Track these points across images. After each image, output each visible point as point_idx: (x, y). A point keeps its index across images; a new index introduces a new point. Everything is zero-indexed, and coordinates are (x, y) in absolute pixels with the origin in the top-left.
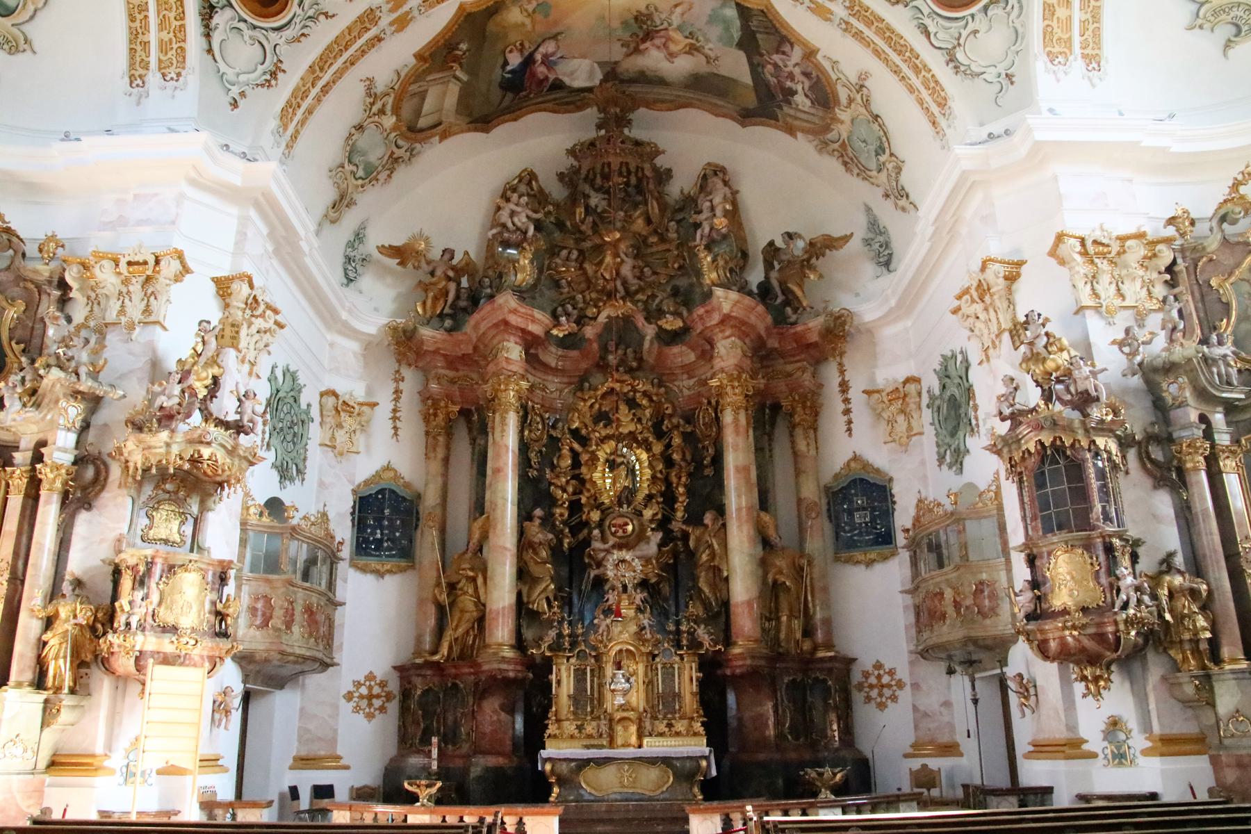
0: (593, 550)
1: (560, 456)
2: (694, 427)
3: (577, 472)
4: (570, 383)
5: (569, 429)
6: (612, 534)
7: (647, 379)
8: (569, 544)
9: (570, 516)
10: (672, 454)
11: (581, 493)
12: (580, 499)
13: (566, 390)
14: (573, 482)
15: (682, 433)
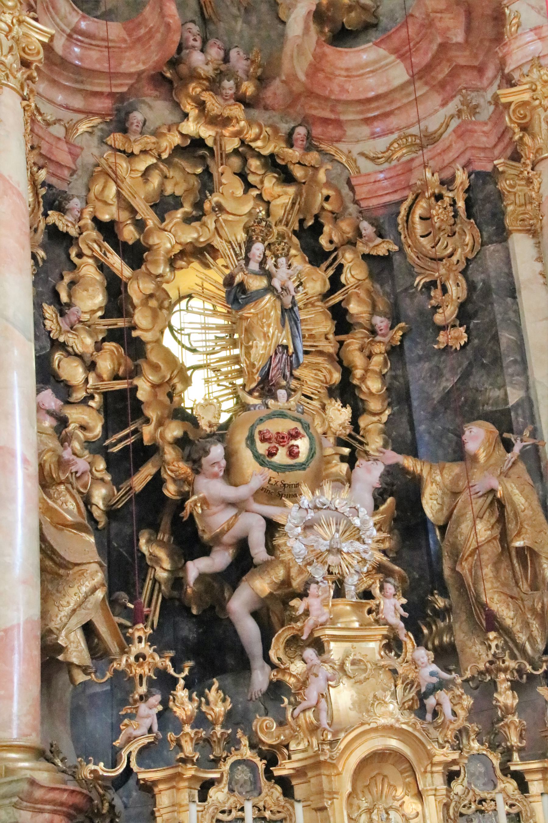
0: (205, 502)
1: (72, 283)
2: (398, 242)
3: (121, 323)
4: (88, 113)
5: (95, 220)
6: (257, 457)
7: (276, 130)
8: (106, 499)
9: (107, 431)
10: (347, 300)
11: (136, 372)
12: (135, 389)
13: (83, 127)
14: (109, 346)
15: (366, 257)
